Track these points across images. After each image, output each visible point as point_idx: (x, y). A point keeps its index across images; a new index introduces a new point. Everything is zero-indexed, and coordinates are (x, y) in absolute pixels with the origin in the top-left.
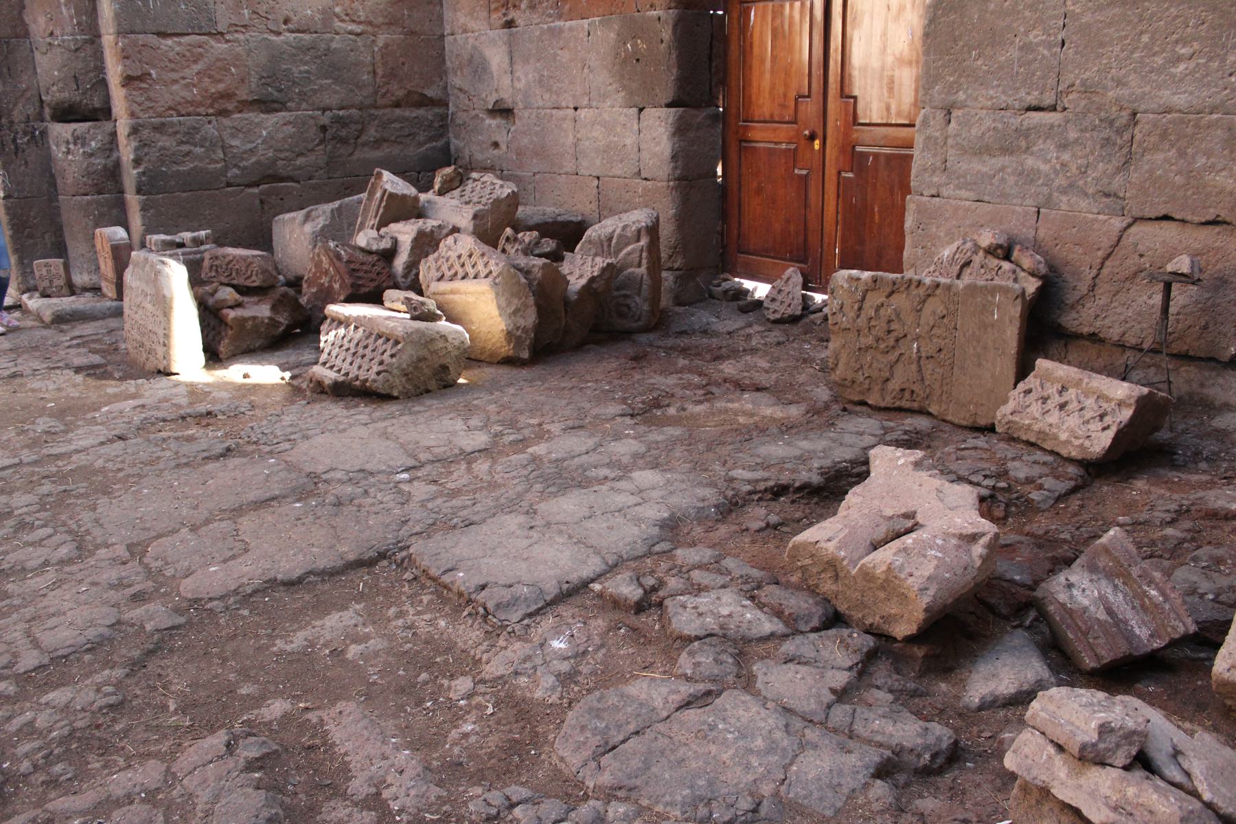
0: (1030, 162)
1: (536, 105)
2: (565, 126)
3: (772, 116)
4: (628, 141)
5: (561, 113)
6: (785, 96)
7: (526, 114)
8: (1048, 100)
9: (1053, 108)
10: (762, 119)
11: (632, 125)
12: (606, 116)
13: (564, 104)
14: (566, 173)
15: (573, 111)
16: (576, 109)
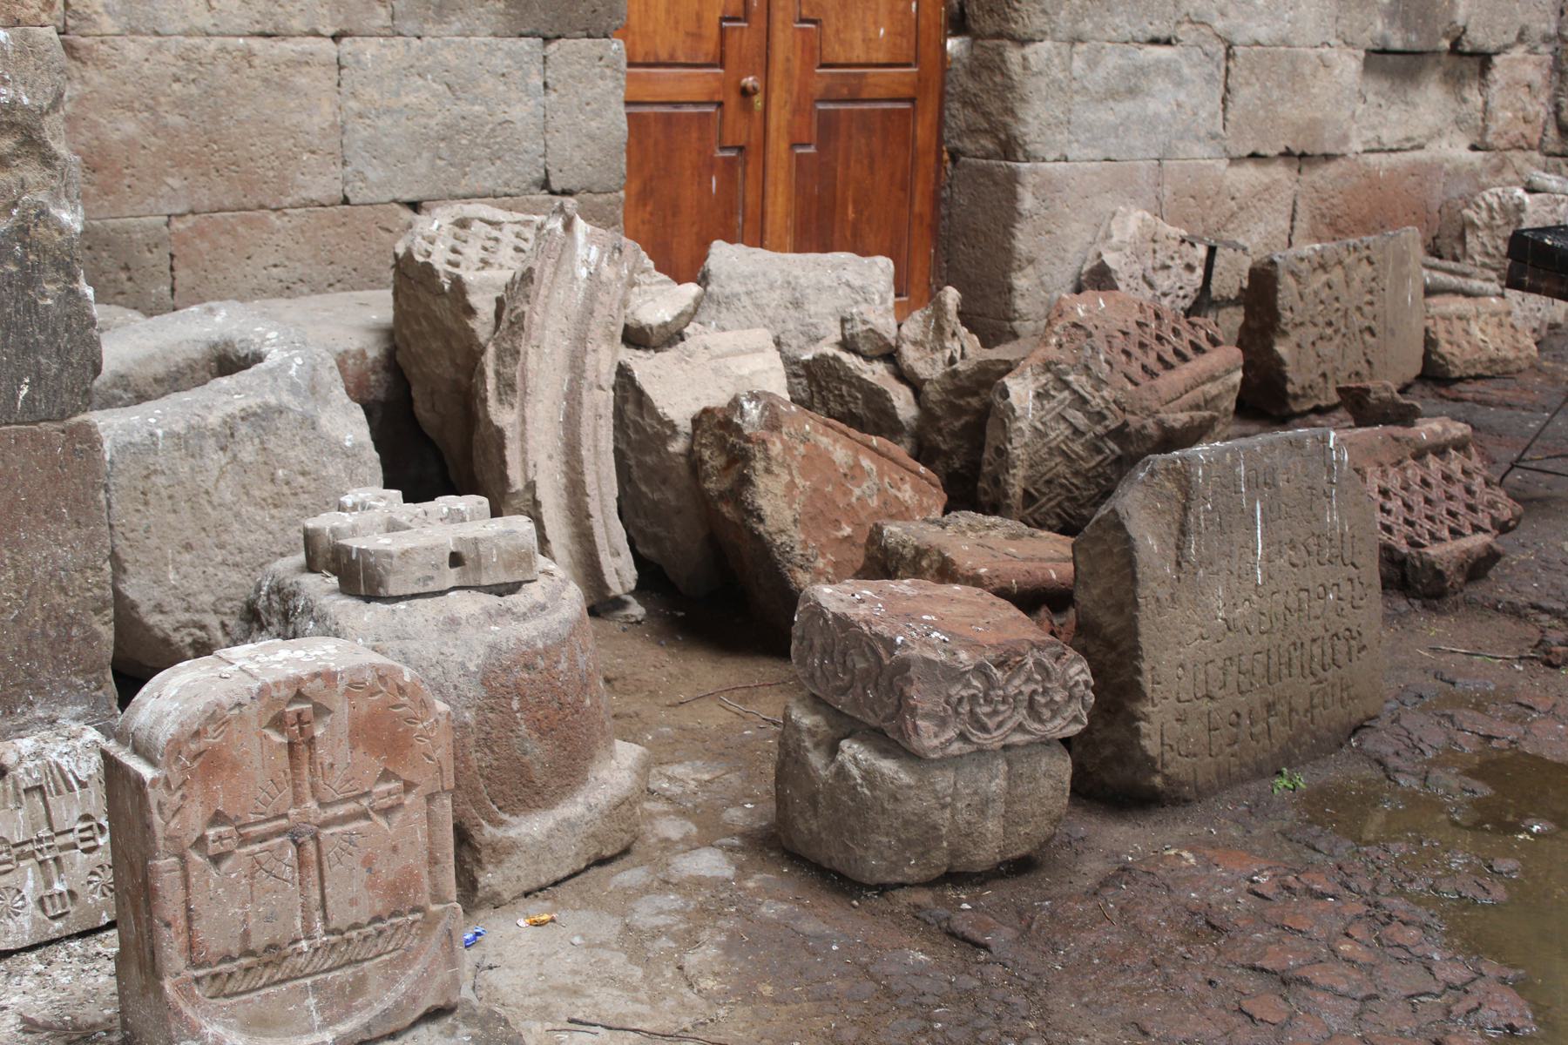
0: (1153, 106)
1: (181, 26)
2: (302, 81)
3: (672, 56)
4: (518, 112)
5: (288, 48)
6: (699, 18)
7: (133, 49)
8: (1163, 32)
9: (1168, 42)
10: (652, 60)
11: (527, 75)
12: (448, 56)
13: (297, 24)
14: (308, 204)
15: (328, 44)
16: (336, 38)
